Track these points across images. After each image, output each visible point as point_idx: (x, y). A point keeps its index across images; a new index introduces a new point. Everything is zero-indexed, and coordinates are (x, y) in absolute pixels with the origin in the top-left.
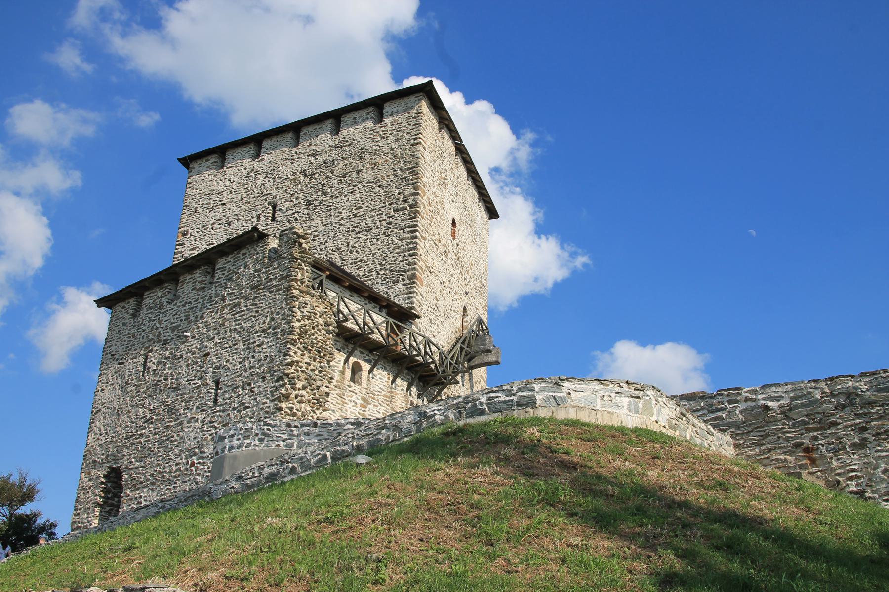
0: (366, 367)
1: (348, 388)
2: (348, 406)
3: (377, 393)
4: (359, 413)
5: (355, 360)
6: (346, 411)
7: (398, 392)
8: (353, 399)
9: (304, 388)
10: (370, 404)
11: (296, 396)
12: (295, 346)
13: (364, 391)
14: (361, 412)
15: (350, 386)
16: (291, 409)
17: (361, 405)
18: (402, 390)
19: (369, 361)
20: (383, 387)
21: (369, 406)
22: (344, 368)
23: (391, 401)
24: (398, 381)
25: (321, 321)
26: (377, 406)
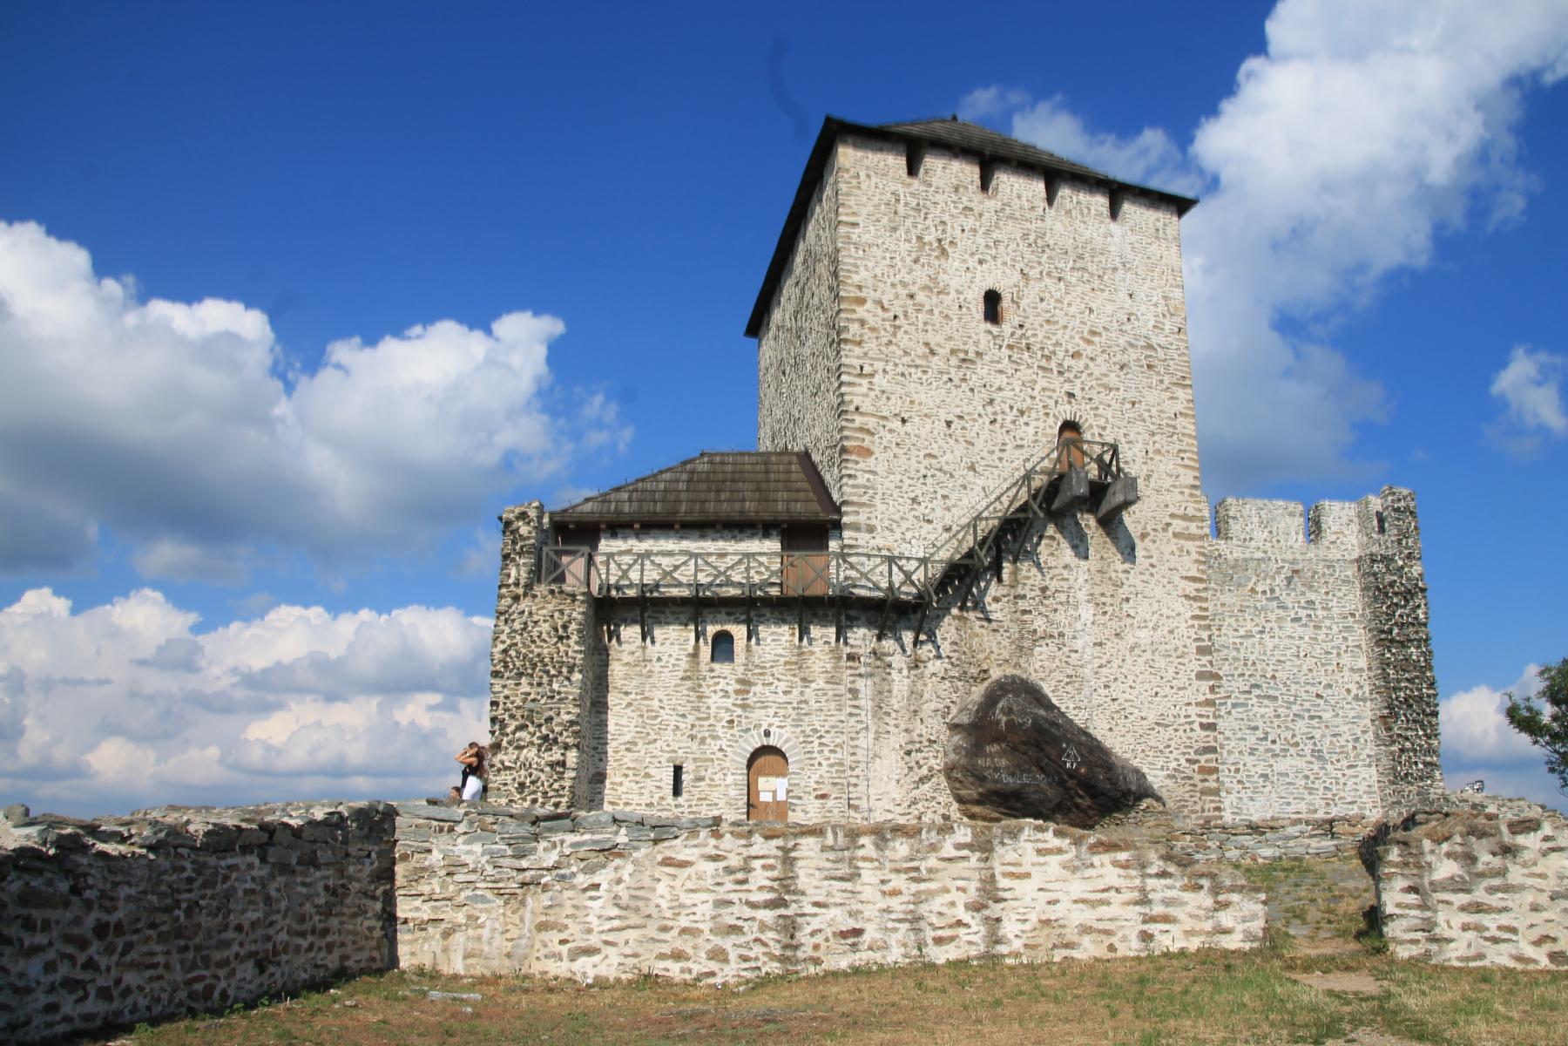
0: (739, 631)
1: (708, 674)
2: (710, 702)
3: (768, 665)
4: (734, 705)
5: (718, 628)
6: (708, 708)
7: (817, 649)
8: (720, 687)
9: (522, 727)
10: (756, 684)
11: (509, 743)
12: (502, 677)
13: (741, 669)
14: (739, 702)
15: (712, 670)
16: (502, 762)
17: (737, 692)
18: (826, 642)
19: (737, 621)
20: (783, 652)
21: (753, 689)
22: (697, 647)
23: (800, 668)
24: (815, 631)
25: (545, 627)
26: (771, 684)
